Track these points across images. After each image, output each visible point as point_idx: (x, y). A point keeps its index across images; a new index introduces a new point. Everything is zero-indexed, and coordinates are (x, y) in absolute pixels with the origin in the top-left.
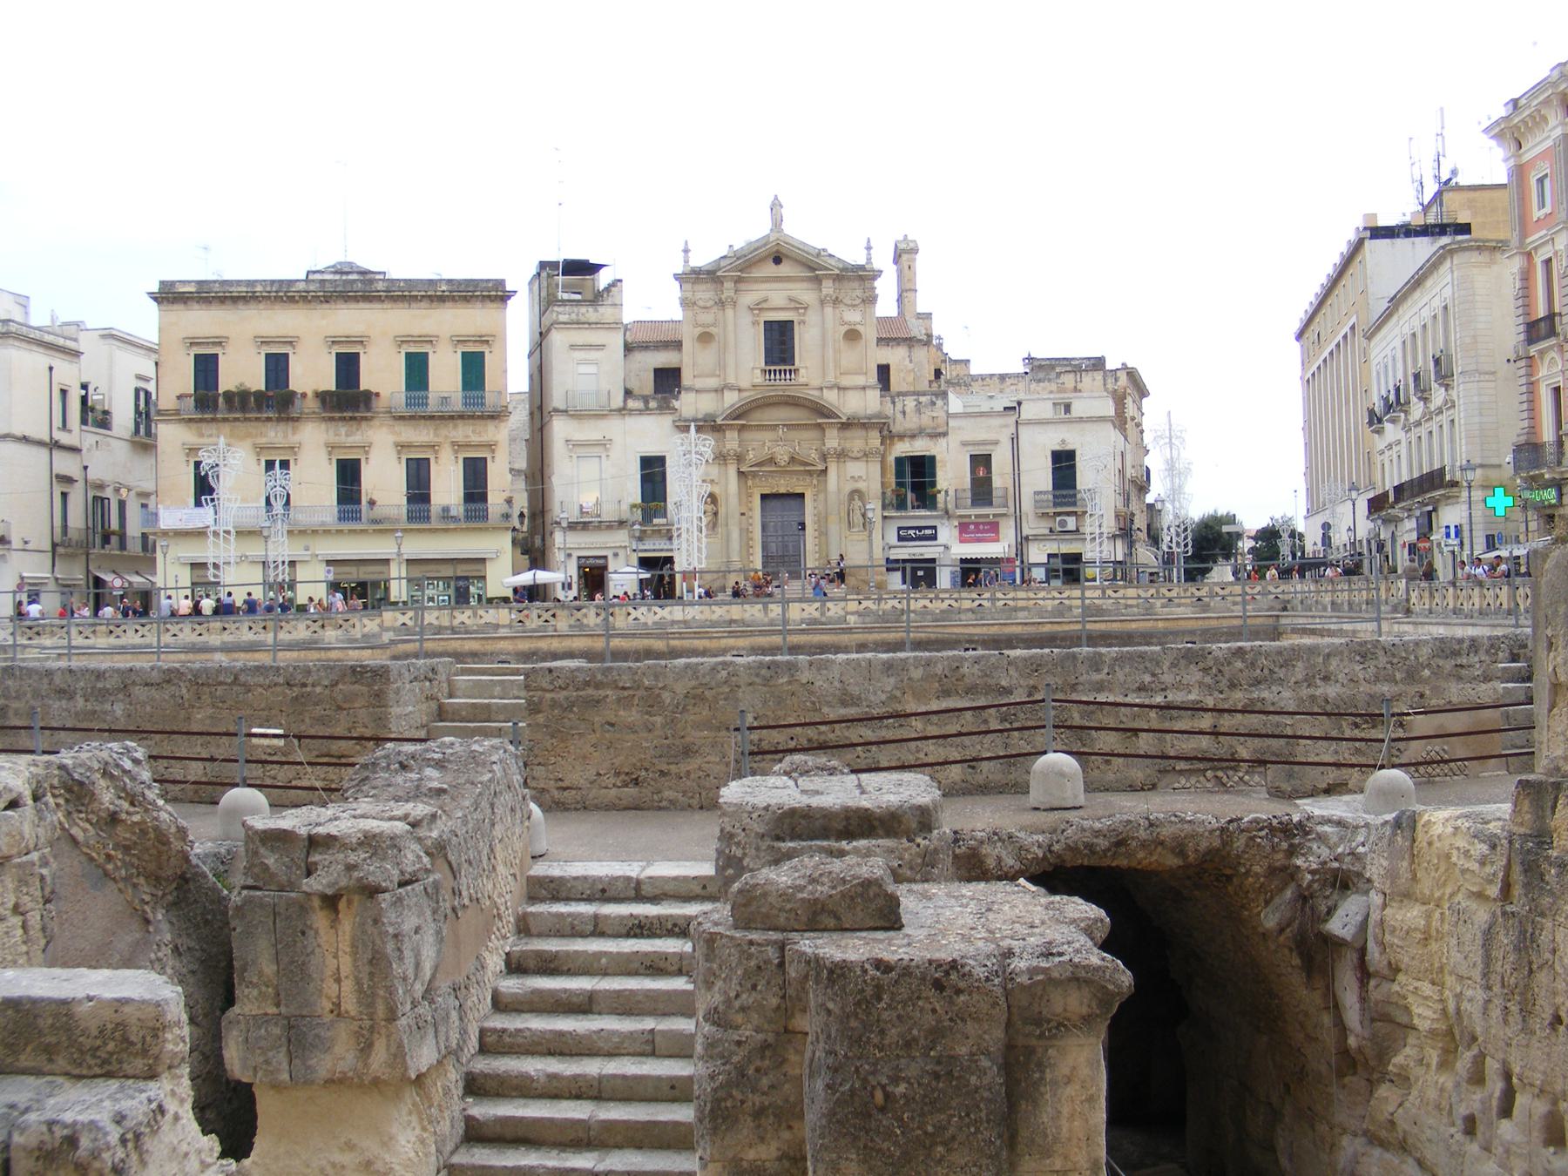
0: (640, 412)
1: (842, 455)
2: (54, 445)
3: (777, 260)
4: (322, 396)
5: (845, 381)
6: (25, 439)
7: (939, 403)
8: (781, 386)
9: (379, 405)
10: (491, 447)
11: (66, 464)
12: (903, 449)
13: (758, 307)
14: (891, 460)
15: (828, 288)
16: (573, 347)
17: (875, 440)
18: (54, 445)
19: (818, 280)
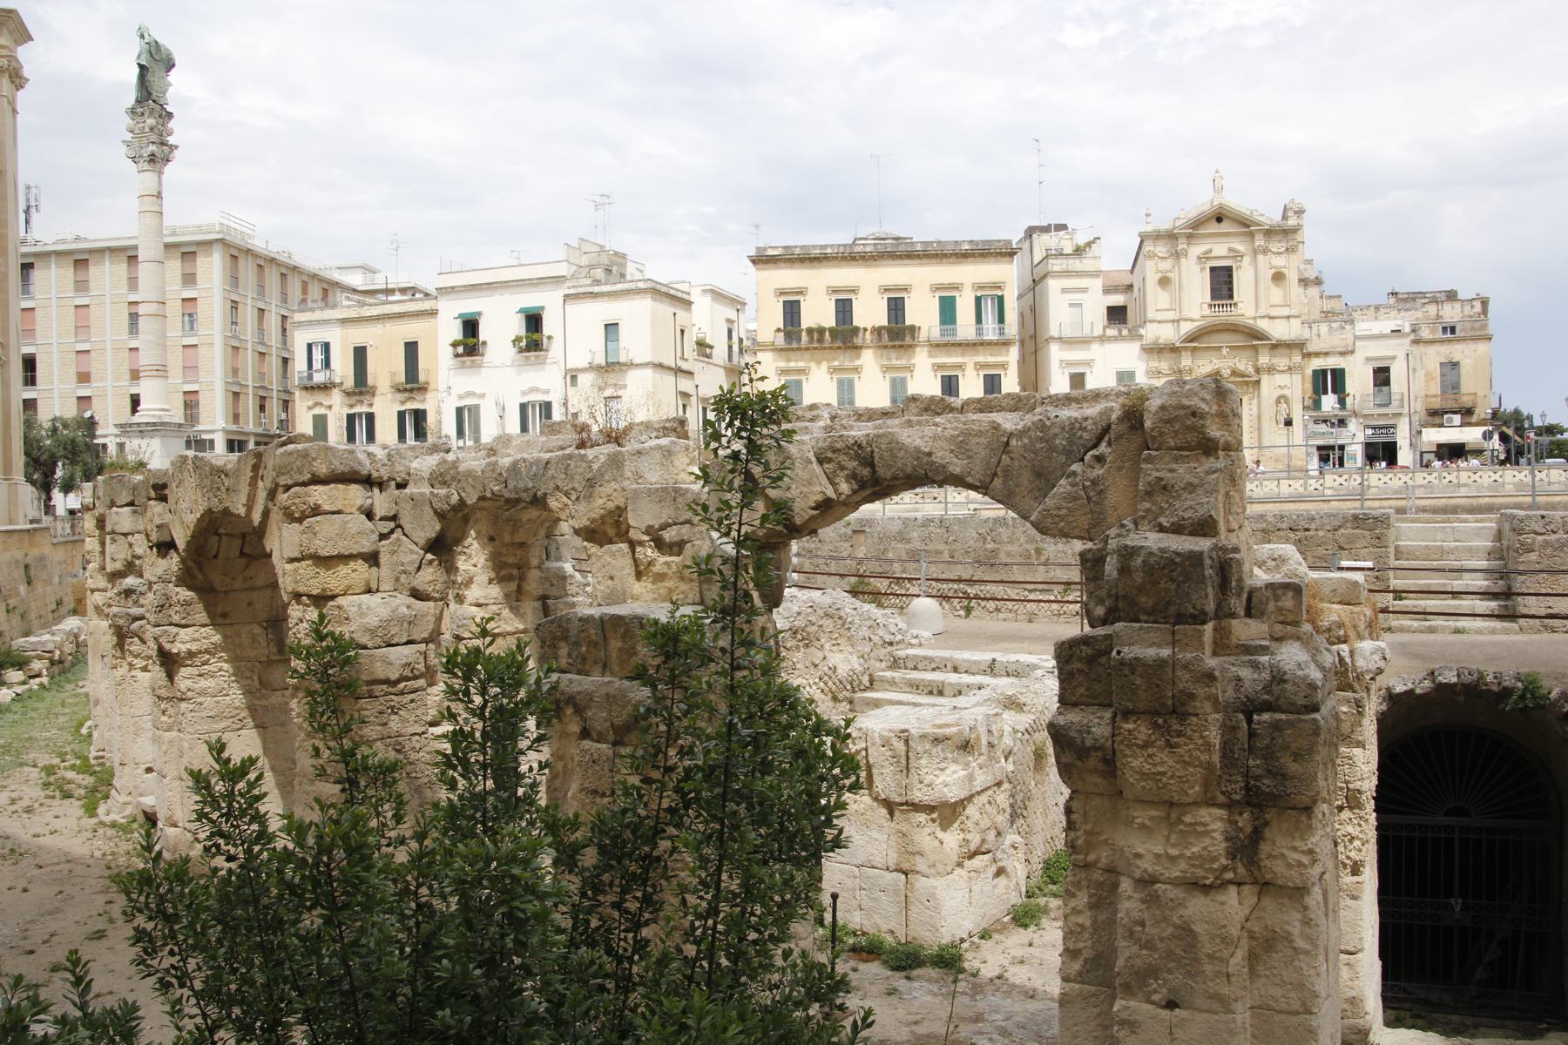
0: (1115, 339)
1: (1271, 370)
2: (678, 371)
3: (1219, 220)
4: (878, 331)
5: (1273, 312)
6: (660, 366)
7: (1348, 327)
8: (1223, 315)
9: (923, 336)
10: (1003, 366)
11: (686, 385)
12: (1317, 363)
13: (1205, 257)
14: (1309, 372)
15: (1260, 241)
16: (1064, 290)
17: (1297, 359)
18: (678, 371)
19: (1252, 235)
